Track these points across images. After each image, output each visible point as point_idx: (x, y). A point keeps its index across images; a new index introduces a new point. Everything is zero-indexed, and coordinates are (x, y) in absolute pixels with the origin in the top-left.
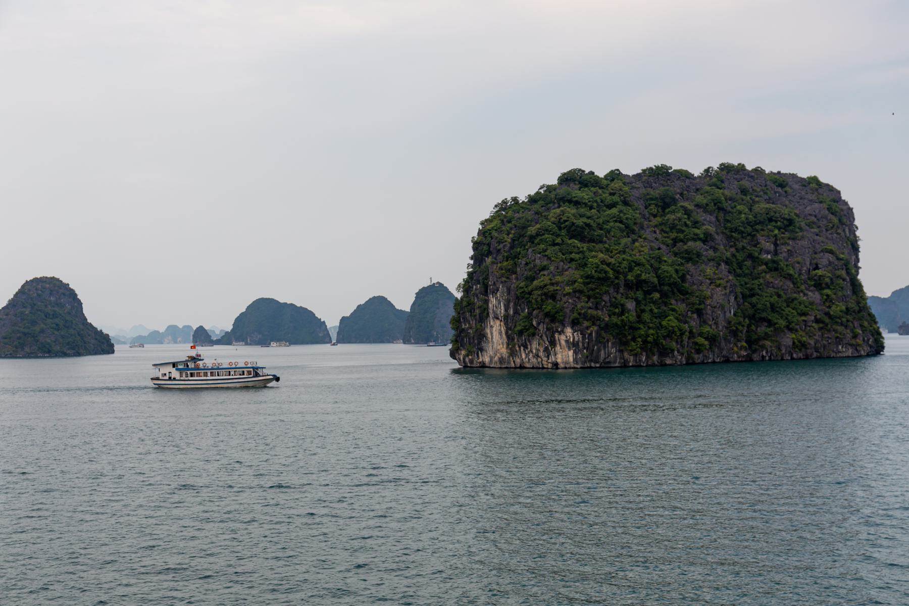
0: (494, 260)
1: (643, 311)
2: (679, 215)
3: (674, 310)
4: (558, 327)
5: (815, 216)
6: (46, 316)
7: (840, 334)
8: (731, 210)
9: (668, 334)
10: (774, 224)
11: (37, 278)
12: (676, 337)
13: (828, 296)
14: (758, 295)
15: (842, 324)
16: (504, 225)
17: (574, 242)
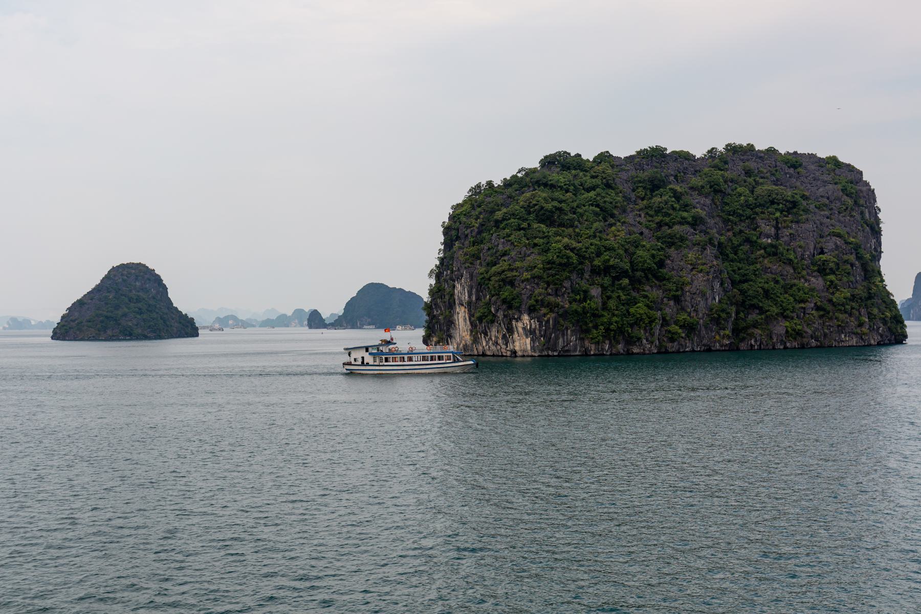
0: (461, 245)
1: (609, 298)
2: (665, 198)
3: (646, 297)
4: (514, 314)
5: (828, 198)
6: (130, 301)
7: (842, 322)
8: (730, 192)
9: (636, 321)
10: (775, 206)
11: (124, 264)
12: (644, 325)
13: (832, 282)
14: (752, 280)
15: (846, 312)
16: (474, 210)
17: (539, 227)
